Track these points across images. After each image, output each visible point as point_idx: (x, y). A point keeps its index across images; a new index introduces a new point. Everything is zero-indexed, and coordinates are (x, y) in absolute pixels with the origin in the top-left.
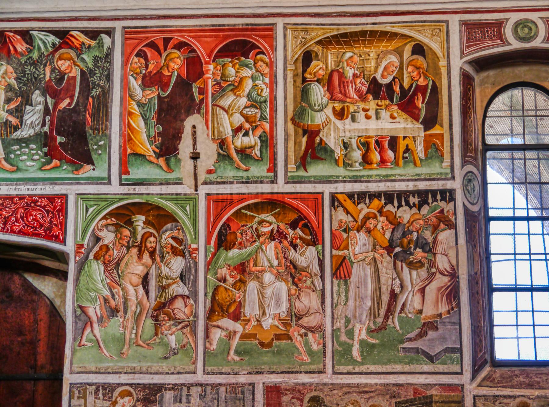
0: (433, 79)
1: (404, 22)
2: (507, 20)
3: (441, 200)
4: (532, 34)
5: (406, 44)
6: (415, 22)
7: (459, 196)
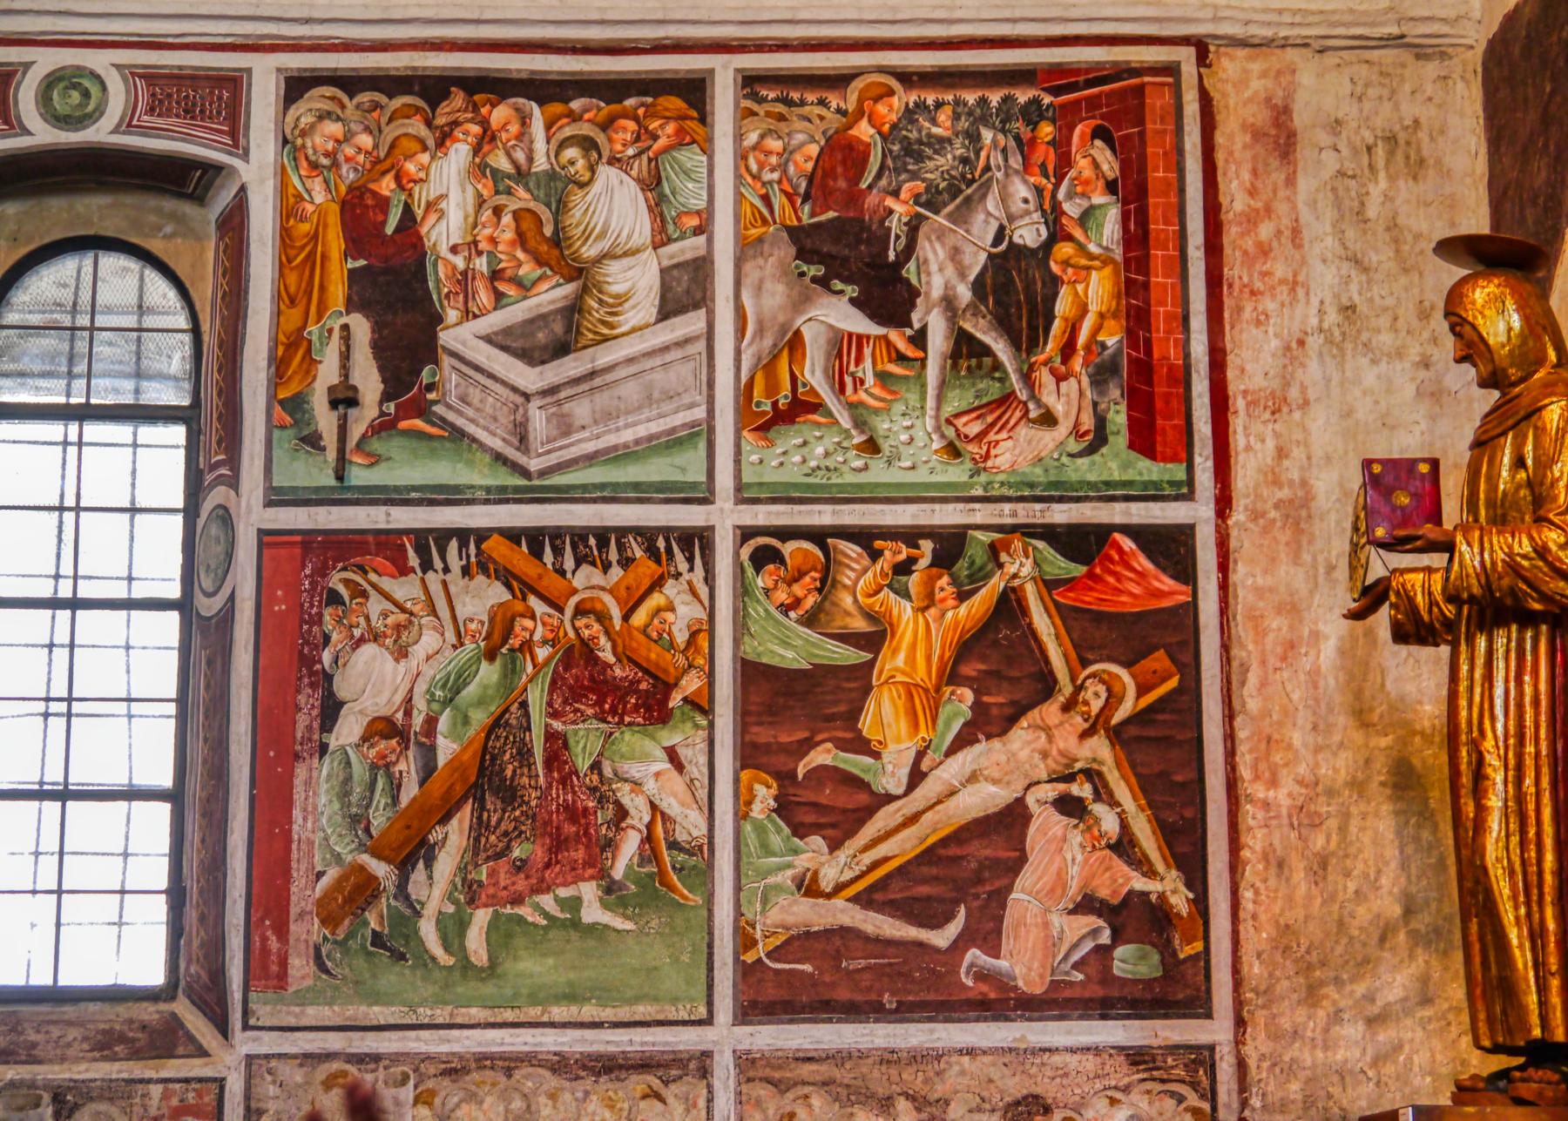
2: (27, 66)
4: (90, 108)
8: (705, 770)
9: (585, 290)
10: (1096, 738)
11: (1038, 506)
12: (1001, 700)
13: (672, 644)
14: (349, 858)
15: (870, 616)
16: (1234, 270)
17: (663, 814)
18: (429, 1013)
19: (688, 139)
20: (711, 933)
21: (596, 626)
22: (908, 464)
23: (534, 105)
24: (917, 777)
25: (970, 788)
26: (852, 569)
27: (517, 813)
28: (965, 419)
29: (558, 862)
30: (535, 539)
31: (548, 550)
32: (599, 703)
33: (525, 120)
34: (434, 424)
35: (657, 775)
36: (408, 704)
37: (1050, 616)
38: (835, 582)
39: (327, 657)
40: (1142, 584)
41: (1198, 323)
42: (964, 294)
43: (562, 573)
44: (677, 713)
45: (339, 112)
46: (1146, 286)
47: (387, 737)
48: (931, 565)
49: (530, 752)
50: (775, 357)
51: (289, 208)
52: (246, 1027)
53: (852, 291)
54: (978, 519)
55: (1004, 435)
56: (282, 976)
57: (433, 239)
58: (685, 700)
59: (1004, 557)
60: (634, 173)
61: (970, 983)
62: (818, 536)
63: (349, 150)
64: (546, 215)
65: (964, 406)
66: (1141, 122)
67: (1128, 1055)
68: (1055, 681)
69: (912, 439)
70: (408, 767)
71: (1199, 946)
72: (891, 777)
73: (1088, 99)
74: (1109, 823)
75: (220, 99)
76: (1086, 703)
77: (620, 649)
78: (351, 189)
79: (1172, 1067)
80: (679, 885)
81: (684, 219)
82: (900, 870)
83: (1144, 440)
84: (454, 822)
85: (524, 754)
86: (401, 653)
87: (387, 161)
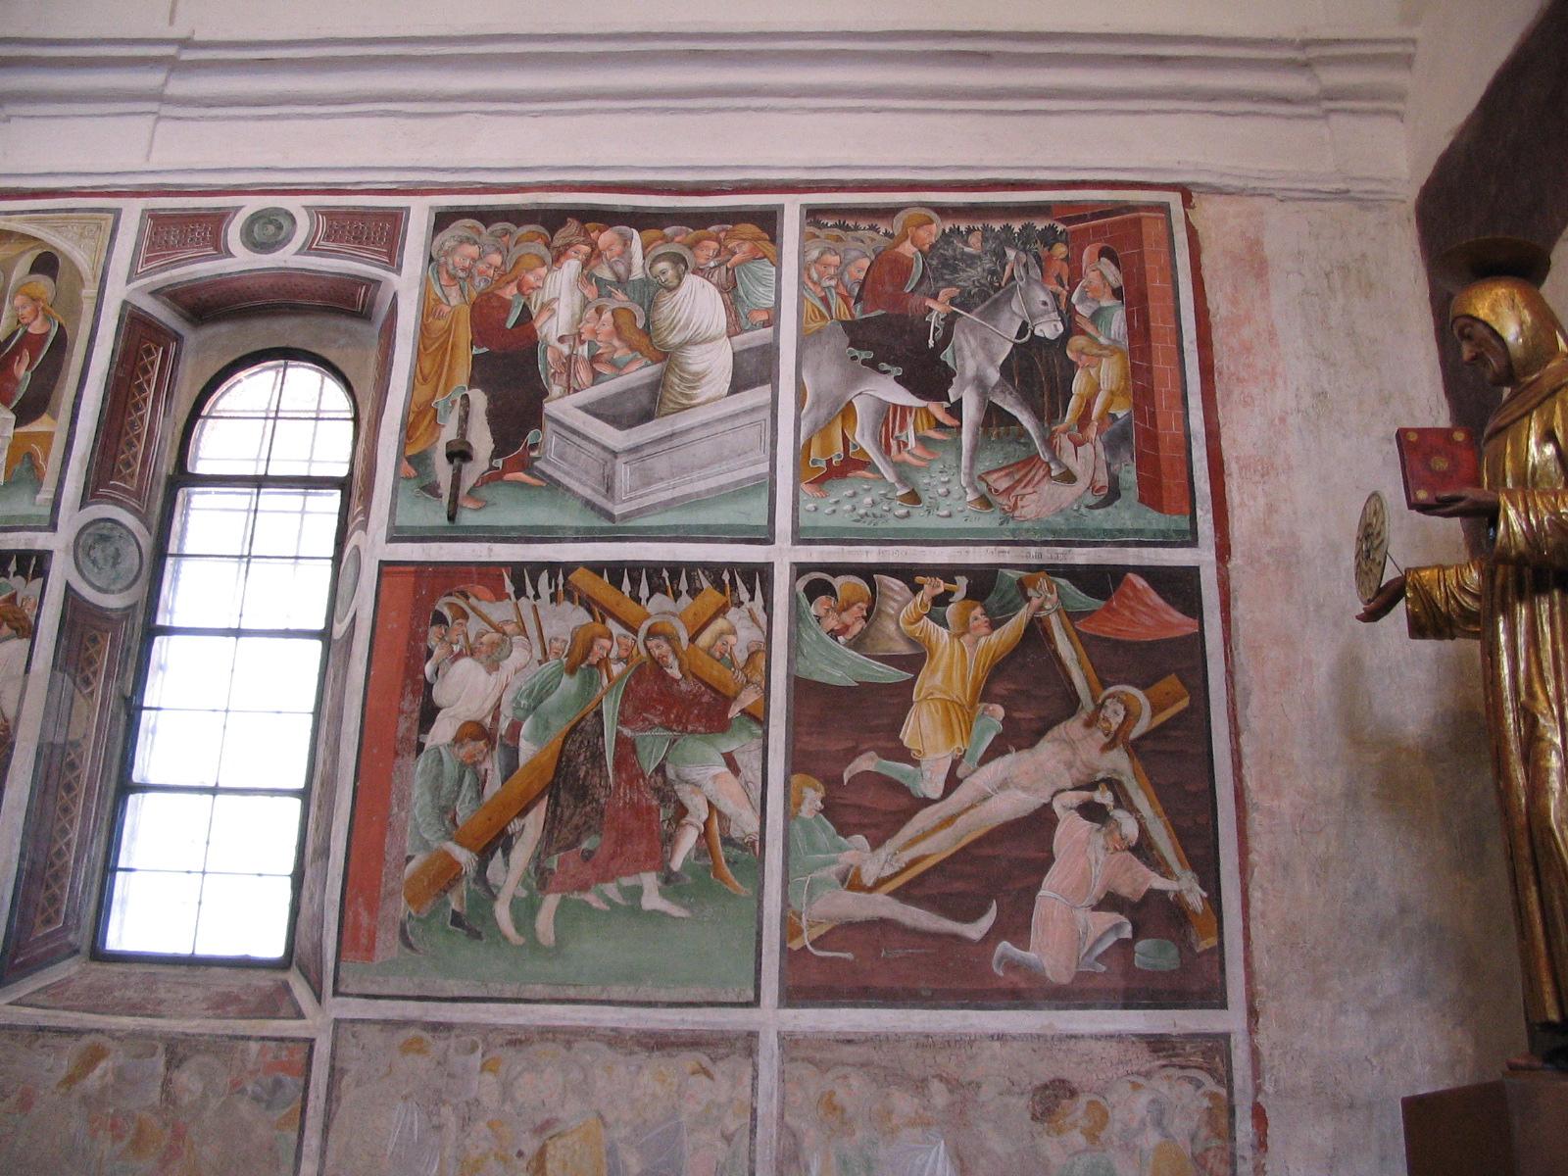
0: (63, 322)
1: (32, 212)
2: (238, 209)
3: (15, 574)
4: (280, 238)
5: (23, 253)
6: (53, 211)
7: (62, 569)
8: (759, 774)
9: (669, 369)
10: (1115, 750)
11: (1060, 550)
12: (1029, 716)
13: (732, 663)
14: (436, 845)
15: (911, 641)
16: (1222, 359)
17: (719, 813)
18: (499, 987)
19: (760, 255)
20: (760, 923)
21: (666, 647)
22: (945, 513)
23: (634, 231)
24: (952, 783)
25: (1002, 795)
26: (895, 600)
27: (588, 809)
28: (995, 476)
29: (622, 854)
30: (614, 571)
31: (626, 580)
32: (666, 713)
33: (626, 242)
34: (535, 477)
35: (716, 777)
36: (497, 707)
37: (1072, 643)
38: (880, 611)
39: (429, 668)
40: (1153, 618)
41: (1195, 402)
42: (994, 376)
43: (638, 600)
44: (736, 723)
45: (476, 238)
46: (1149, 370)
47: (475, 738)
48: (966, 598)
49: (602, 754)
50: (830, 423)
51: (428, 310)
52: (336, 993)
53: (898, 371)
54: (1007, 559)
55: (1029, 489)
56: (370, 949)
57: (545, 330)
58: (743, 711)
59: (1031, 592)
60: (715, 279)
61: (1001, 974)
62: (866, 572)
63: (481, 266)
64: (639, 312)
65: (995, 466)
66: (1140, 244)
67: (1149, 1043)
68: (1078, 699)
69: (949, 492)
70: (493, 767)
71: (1213, 941)
72: (932, 787)
73: (1093, 227)
74: (1130, 828)
75: (380, 232)
76: (1106, 719)
77: (686, 667)
78: (480, 295)
79: (1190, 1055)
80: (732, 877)
81: (755, 314)
82: (935, 868)
83: (1152, 494)
84: (531, 816)
85: (597, 756)
86: (493, 666)
87: (512, 273)
